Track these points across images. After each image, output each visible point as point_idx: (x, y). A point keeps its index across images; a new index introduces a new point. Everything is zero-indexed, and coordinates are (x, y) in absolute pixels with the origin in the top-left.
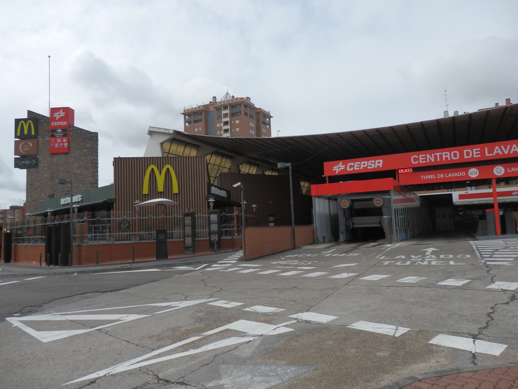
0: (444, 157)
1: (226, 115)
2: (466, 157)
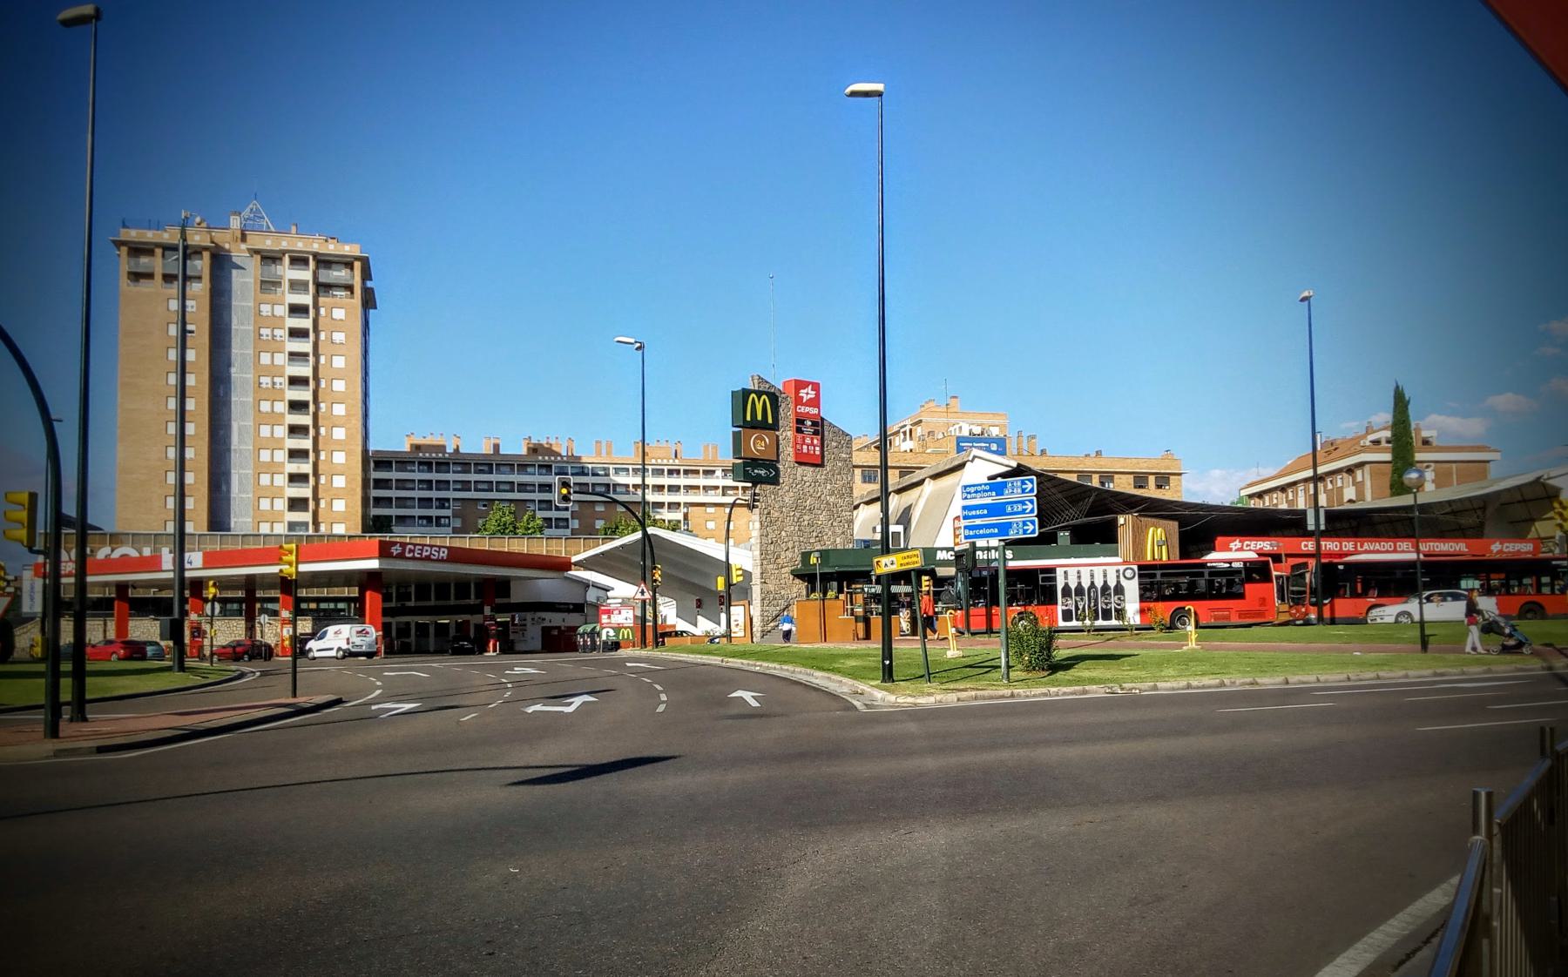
0: (1328, 546)
1: (296, 286)
2: (1344, 549)
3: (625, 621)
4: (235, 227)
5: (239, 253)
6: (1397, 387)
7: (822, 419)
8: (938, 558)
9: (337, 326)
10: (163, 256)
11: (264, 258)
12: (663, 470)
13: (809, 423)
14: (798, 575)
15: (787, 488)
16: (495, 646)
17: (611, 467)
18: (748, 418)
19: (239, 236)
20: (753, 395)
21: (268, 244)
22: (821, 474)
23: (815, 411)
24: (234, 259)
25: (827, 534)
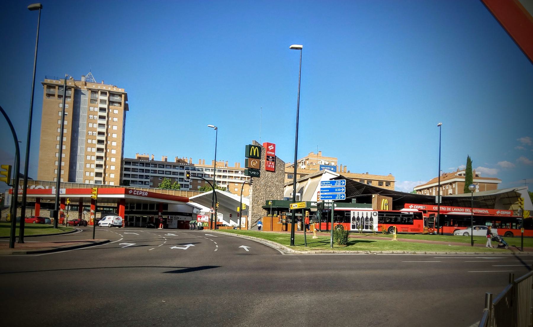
0: (442, 209)
1: (102, 101)
2: (447, 210)
3: (206, 220)
4: (83, 81)
5: (84, 89)
6: (468, 157)
7: (276, 156)
8: (311, 205)
9: (115, 116)
10: (58, 89)
11: (92, 92)
12: (221, 170)
13: (271, 157)
14: (264, 208)
15: (262, 179)
16: (162, 226)
17: (204, 168)
18: (251, 155)
19: (84, 84)
20: (253, 147)
21: (94, 87)
22: (274, 175)
23: (273, 153)
24: (82, 91)
25: (275, 195)
